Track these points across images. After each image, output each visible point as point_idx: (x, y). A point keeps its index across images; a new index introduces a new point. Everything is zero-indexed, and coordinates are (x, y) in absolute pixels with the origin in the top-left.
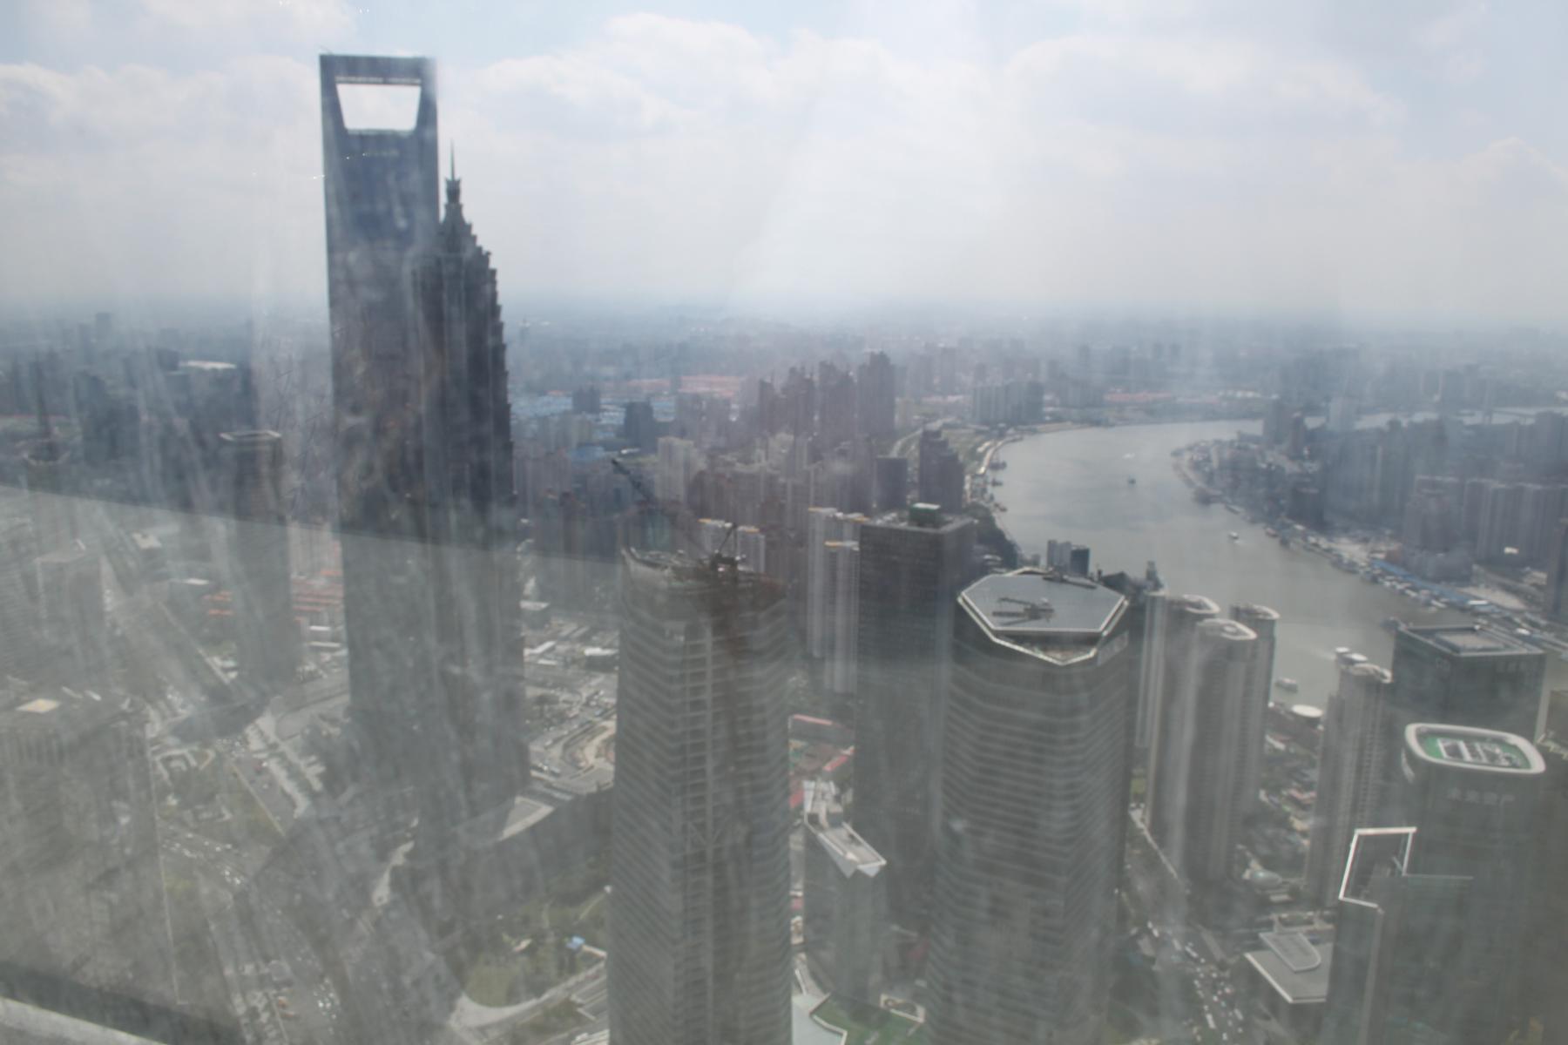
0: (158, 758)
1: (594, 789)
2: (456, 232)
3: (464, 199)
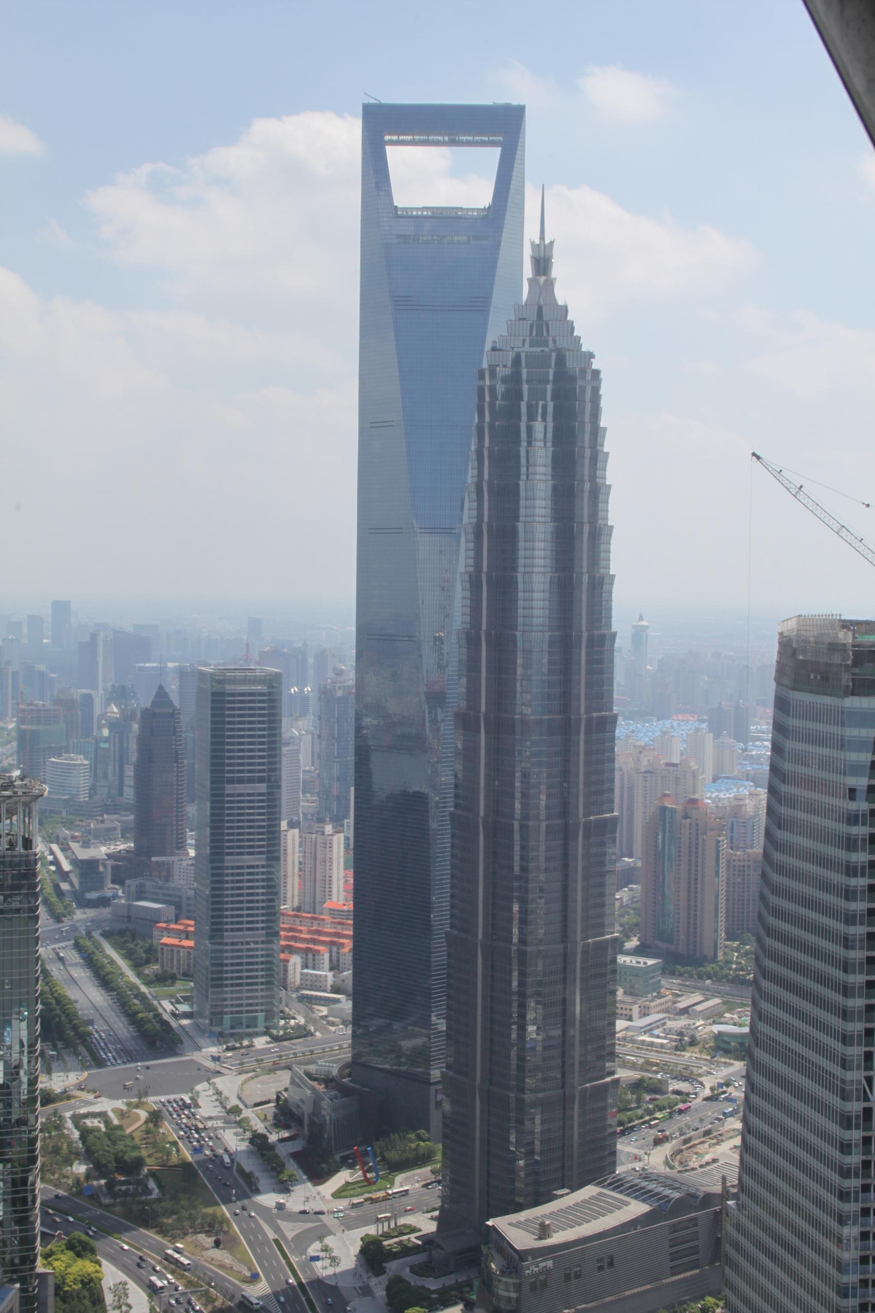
0: (68, 1115)
1: (718, 1189)
2: (545, 320)
3: (557, 271)
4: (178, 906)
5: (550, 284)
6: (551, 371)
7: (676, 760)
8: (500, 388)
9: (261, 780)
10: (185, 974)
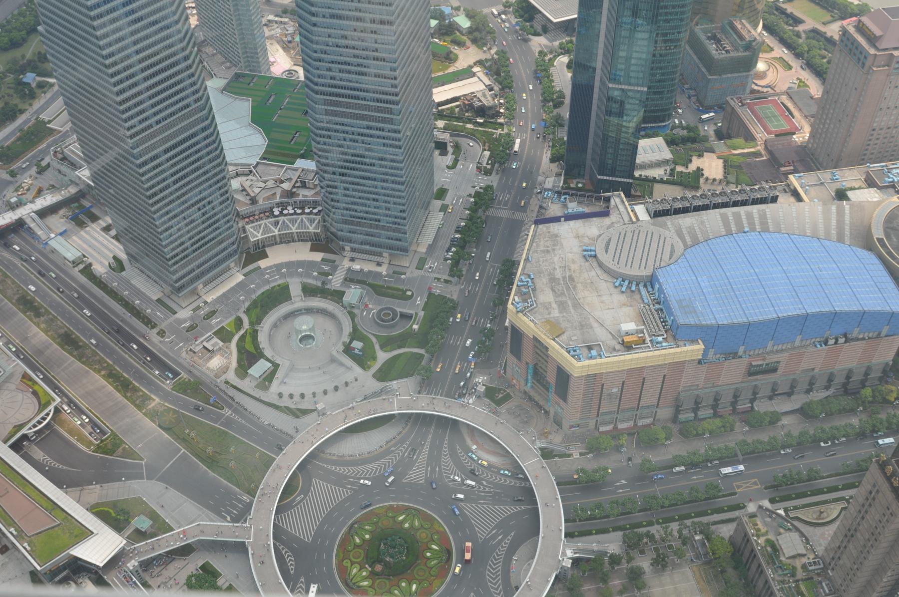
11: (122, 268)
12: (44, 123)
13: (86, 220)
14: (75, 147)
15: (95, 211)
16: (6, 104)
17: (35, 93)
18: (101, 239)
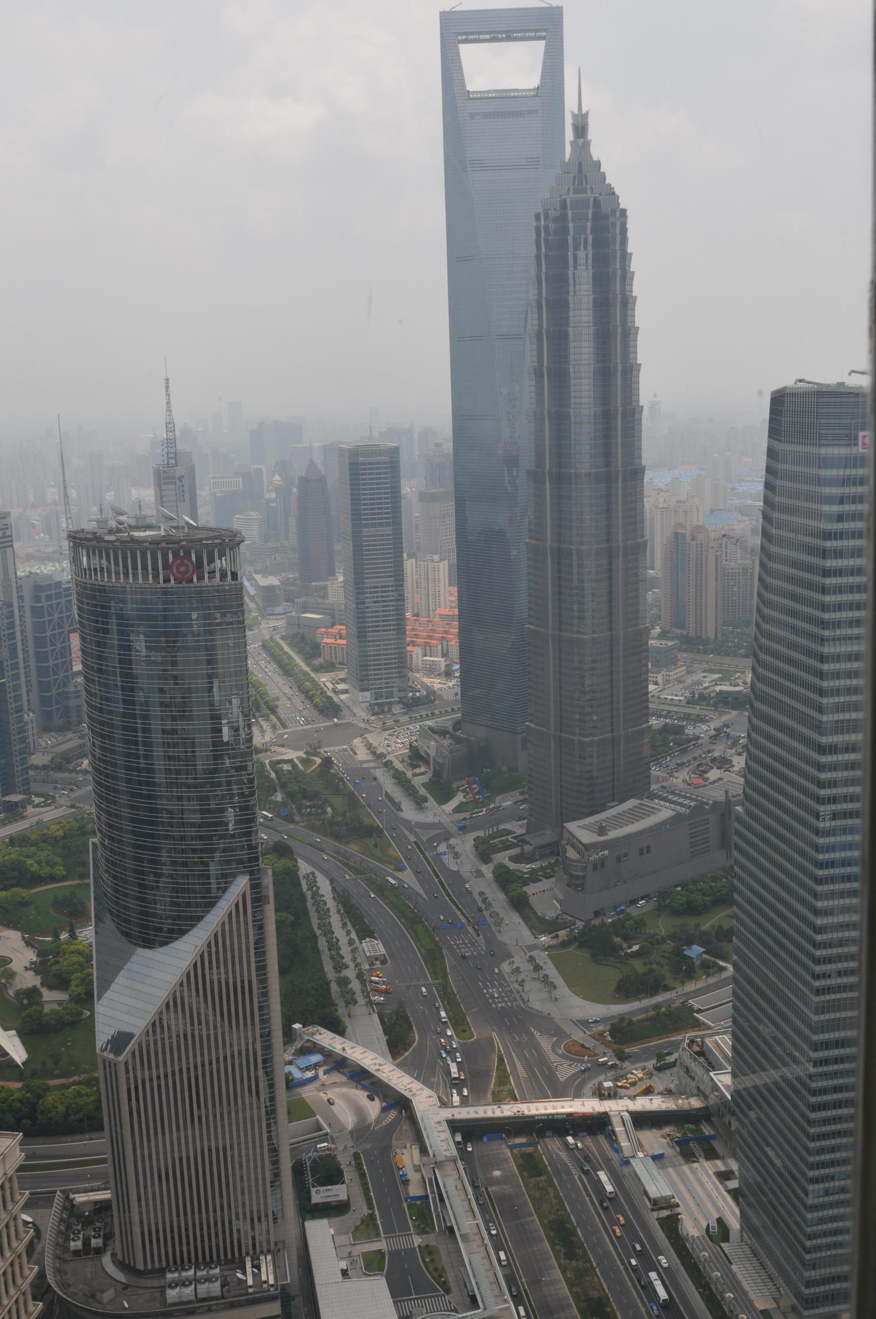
0: (267, 762)
2: (585, 172)
3: (591, 134)
4: (333, 616)
5: (587, 145)
6: (590, 212)
7: (683, 497)
8: (552, 226)
9: (388, 524)
10: (340, 664)
11: (726, 1239)
12: (691, 1010)
13: (698, 1151)
14: (723, 1040)
15: (717, 1145)
16: (651, 971)
17: (694, 972)
18: (709, 1186)
